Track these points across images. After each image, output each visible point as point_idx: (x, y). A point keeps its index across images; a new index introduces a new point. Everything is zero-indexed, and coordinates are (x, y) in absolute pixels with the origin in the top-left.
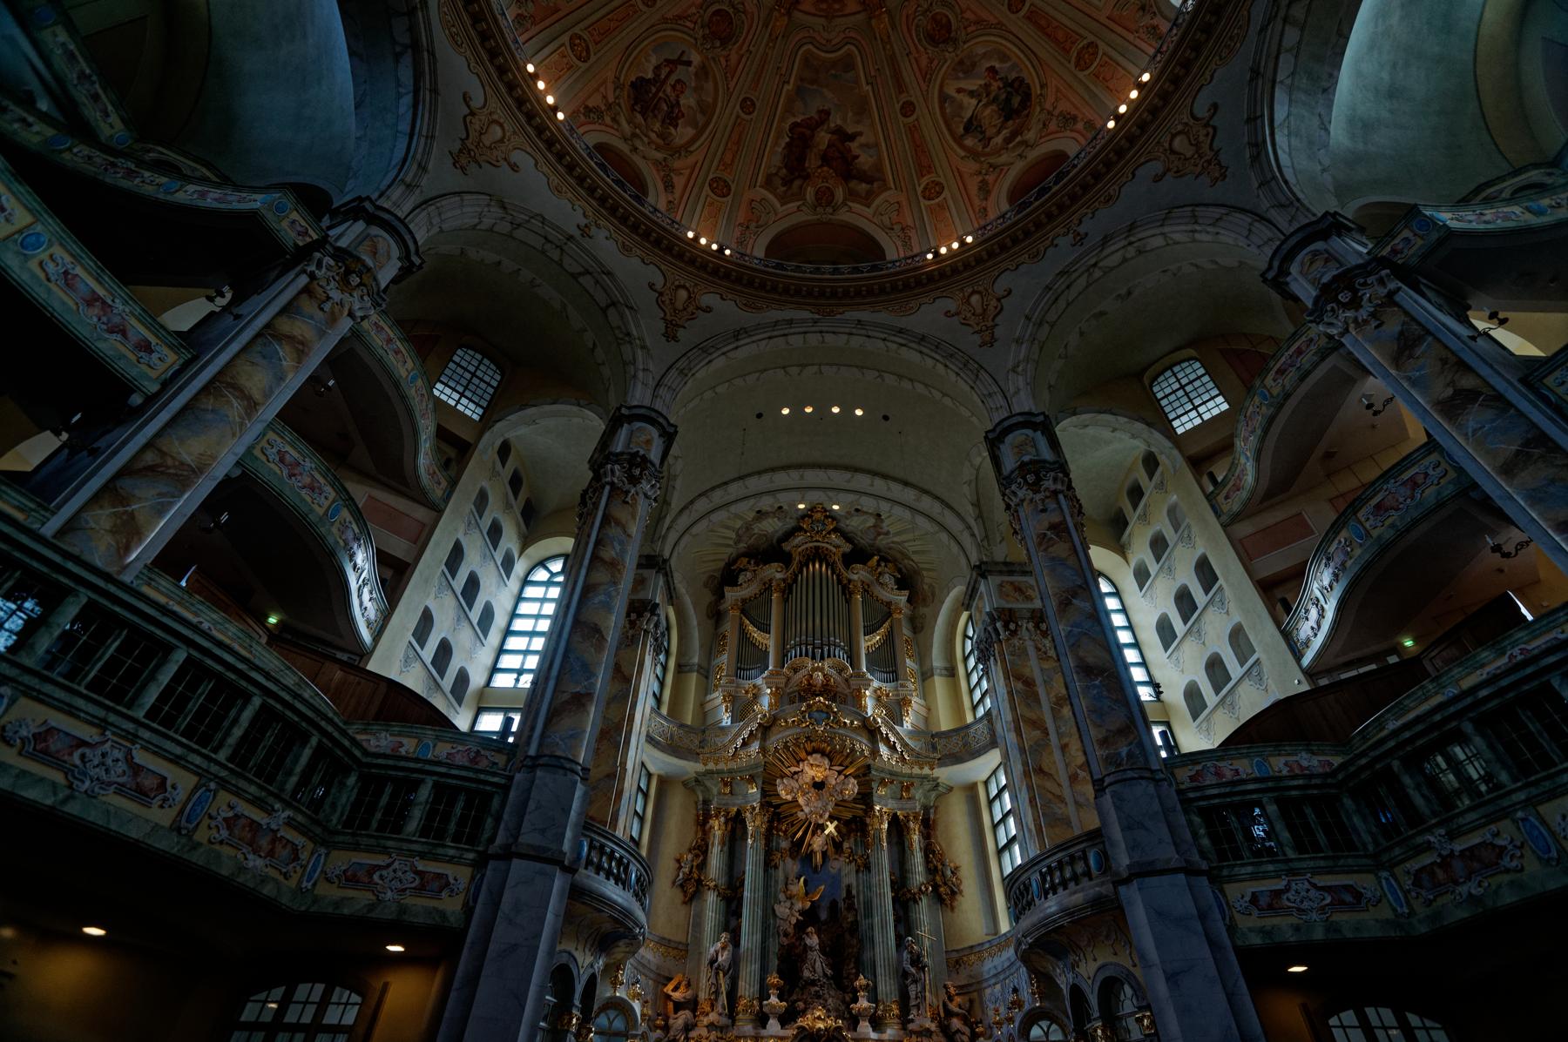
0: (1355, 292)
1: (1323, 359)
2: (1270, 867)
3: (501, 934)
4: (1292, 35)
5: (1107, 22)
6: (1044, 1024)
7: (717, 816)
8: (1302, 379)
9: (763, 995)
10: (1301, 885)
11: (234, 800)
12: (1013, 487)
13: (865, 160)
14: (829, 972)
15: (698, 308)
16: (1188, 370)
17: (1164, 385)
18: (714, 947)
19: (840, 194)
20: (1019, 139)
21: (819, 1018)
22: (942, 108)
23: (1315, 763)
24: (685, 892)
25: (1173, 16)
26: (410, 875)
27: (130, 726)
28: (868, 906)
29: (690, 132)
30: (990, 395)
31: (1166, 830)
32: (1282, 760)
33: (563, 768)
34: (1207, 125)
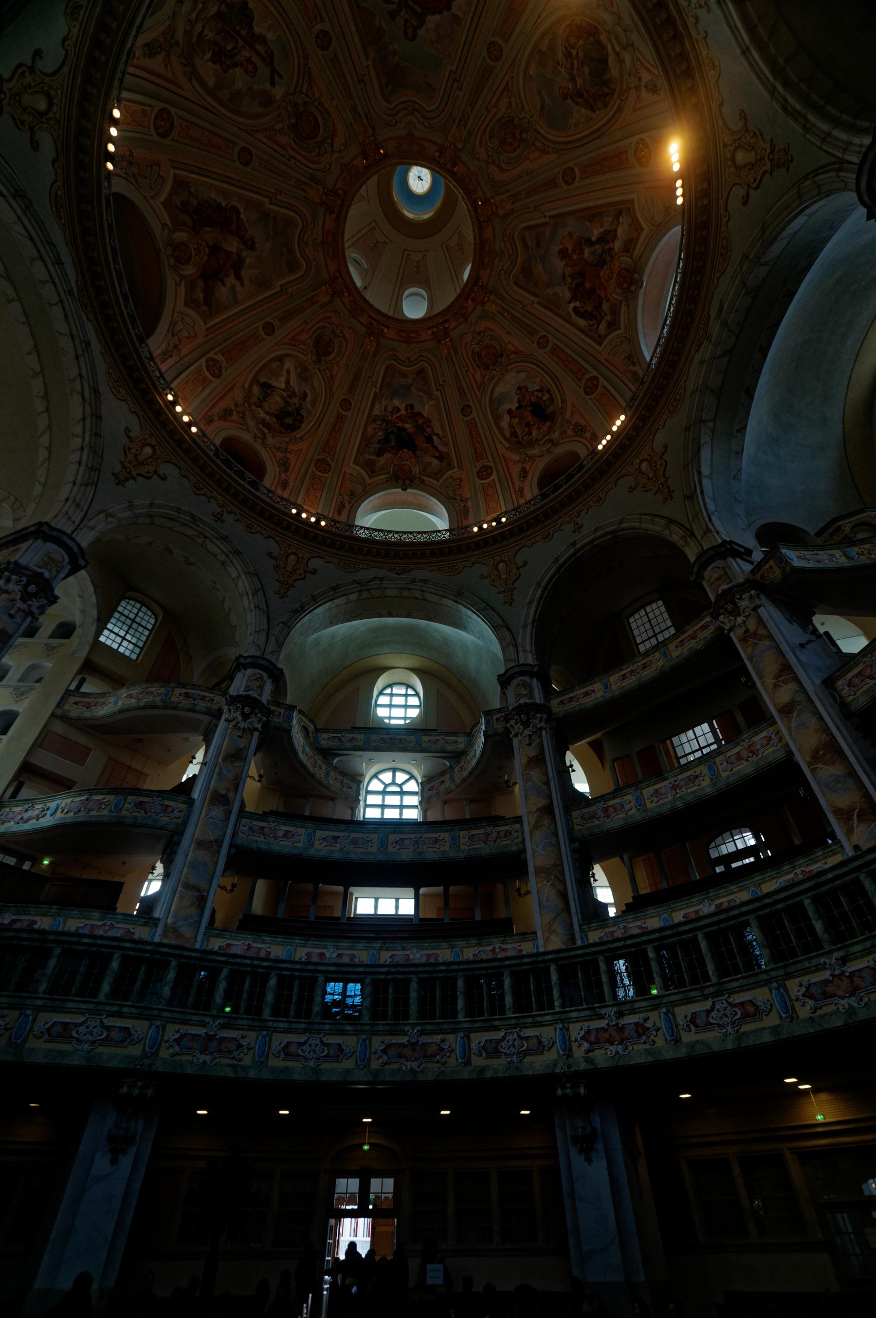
0: (251, 713)
1: (205, 714)
4: (353, 597)
5: (343, 472)
8: (189, 710)
12: (14, 577)
13: (222, 292)
15: (32, 129)
16: (146, 618)
17: (129, 607)
19: (189, 270)
20: (266, 431)
22: (272, 360)
25: (350, 523)
29: (211, 81)
30: (78, 505)
34: (305, 572)
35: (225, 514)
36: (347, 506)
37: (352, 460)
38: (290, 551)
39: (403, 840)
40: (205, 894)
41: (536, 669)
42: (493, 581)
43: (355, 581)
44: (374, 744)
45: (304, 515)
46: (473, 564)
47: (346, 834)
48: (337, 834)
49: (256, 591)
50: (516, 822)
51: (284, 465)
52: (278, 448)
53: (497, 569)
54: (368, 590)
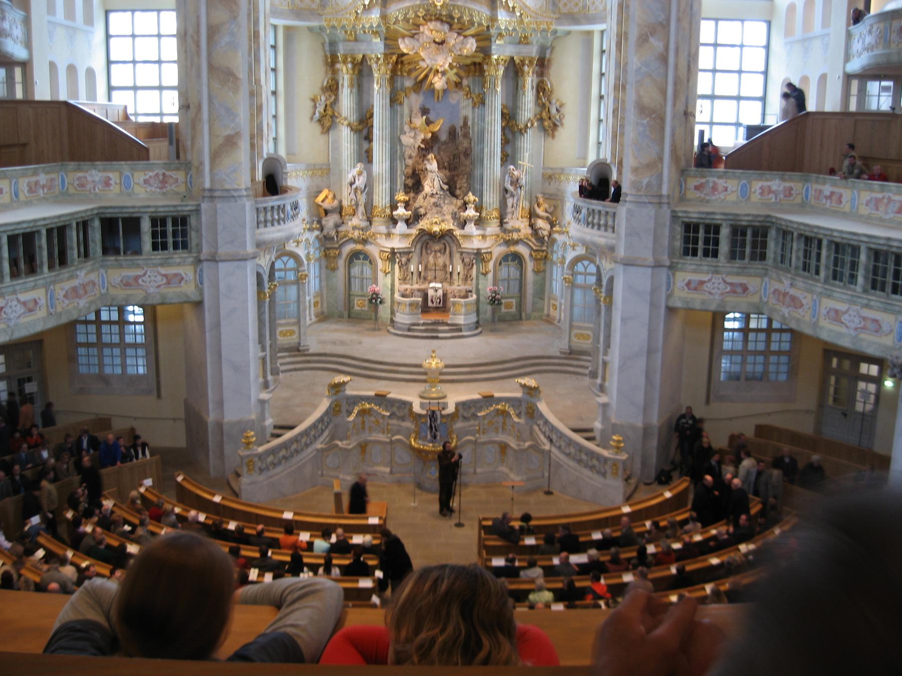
2: (705, 268)
3: (225, 305)
6: (586, 263)
7: (345, 62)
9: (394, 207)
10: (717, 279)
11: (63, 284)
14: (445, 187)
18: (351, 171)
21: (436, 223)
23: (781, 188)
24: (323, 125)
26: (159, 278)
27: (11, 289)
28: (481, 140)
31: (651, 238)
32: (760, 184)
33: (233, 197)
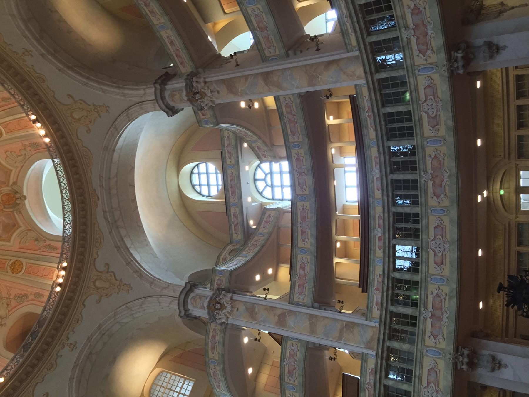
0: (219, 303)
1: (225, 334)
5: (19, 250)
34: (108, 272)
35: (69, 342)
36: (48, 242)
37: (7, 243)
38: (93, 287)
39: (299, 184)
40: (345, 323)
41: (158, 86)
42: (91, 122)
43: (110, 233)
44: (237, 200)
45: (61, 280)
46: (79, 139)
47: (299, 225)
48: (300, 232)
49: (129, 308)
50: (279, 100)
51: (22, 297)
52: (8, 305)
53: (79, 119)
54: (116, 222)
